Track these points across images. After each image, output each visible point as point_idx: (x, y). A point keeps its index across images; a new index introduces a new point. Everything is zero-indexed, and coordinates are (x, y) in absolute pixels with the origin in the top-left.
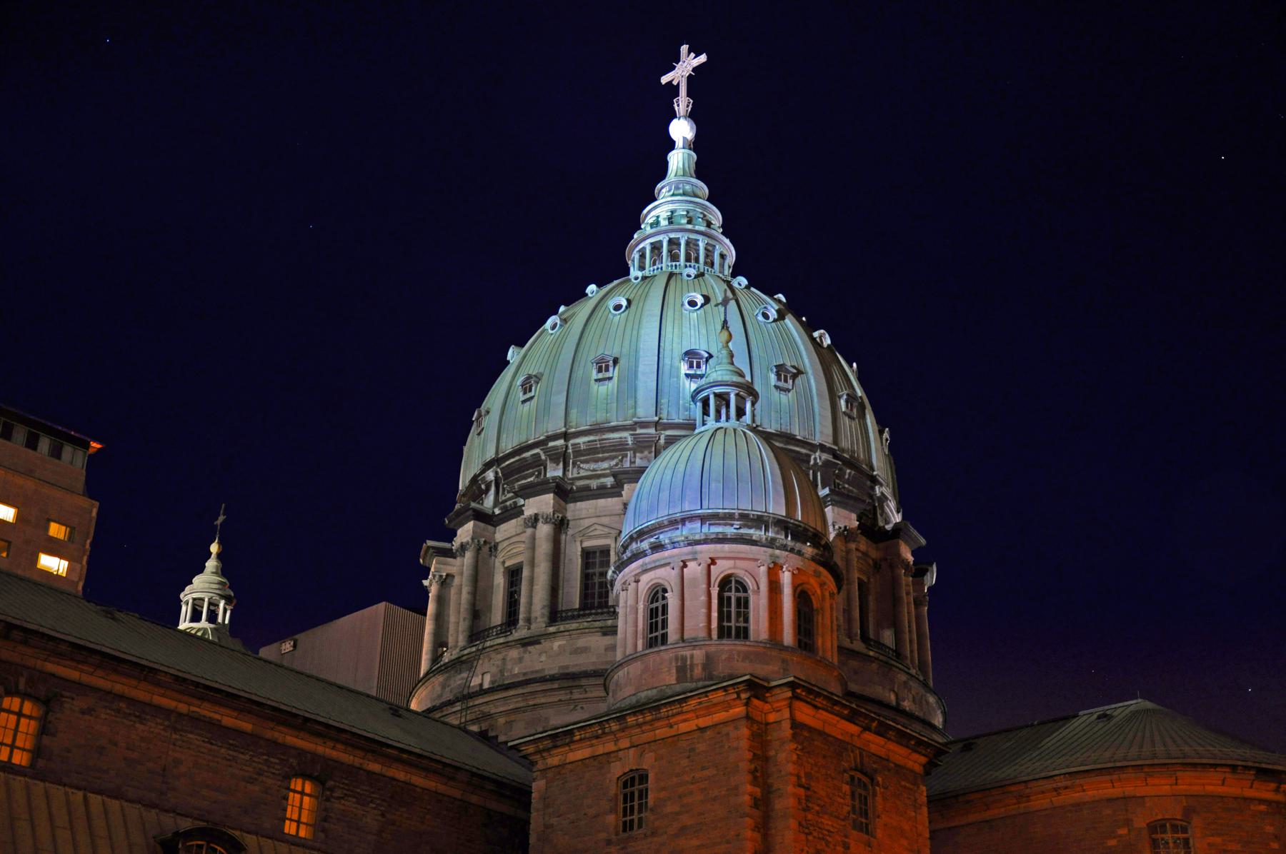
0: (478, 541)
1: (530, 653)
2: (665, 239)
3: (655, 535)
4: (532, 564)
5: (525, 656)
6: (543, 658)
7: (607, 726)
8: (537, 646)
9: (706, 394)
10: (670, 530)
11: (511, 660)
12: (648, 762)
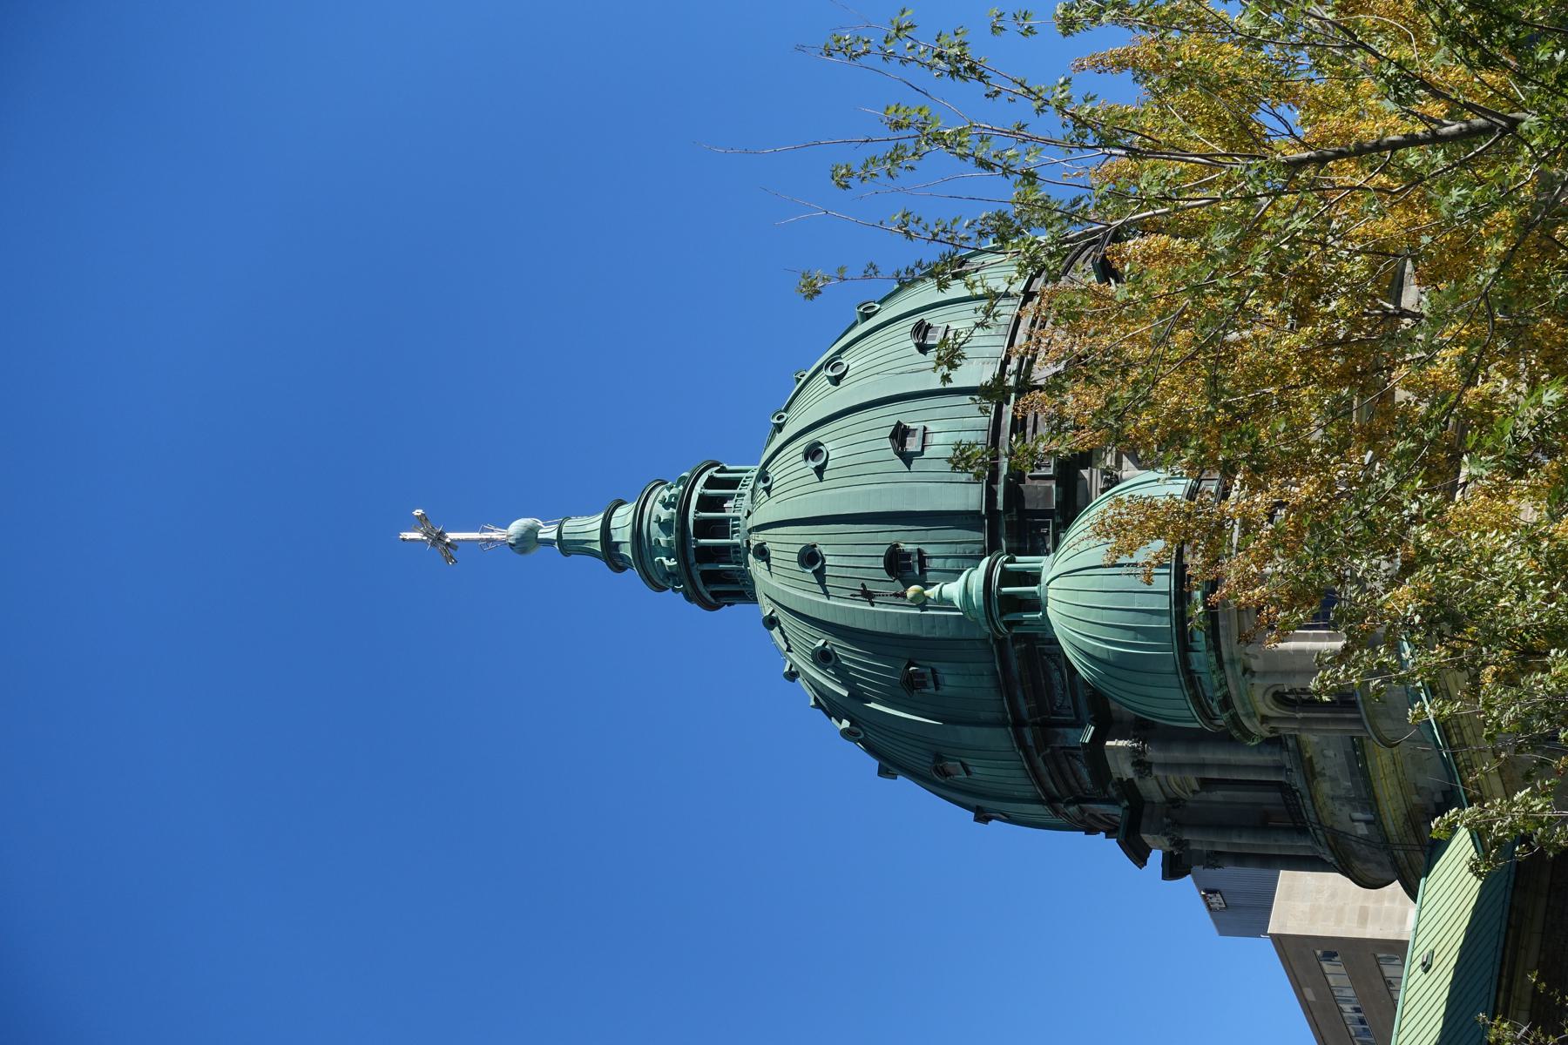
0: (1168, 825)
1: (1324, 769)
2: (697, 570)
3: (1207, 701)
4: (1203, 766)
5: (1328, 774)
6: (1330, 753)
7: (1463, 764)
8: (1315, 760)
9: (1003, 626)
10: (1201, 686)
11: (1332, 790)
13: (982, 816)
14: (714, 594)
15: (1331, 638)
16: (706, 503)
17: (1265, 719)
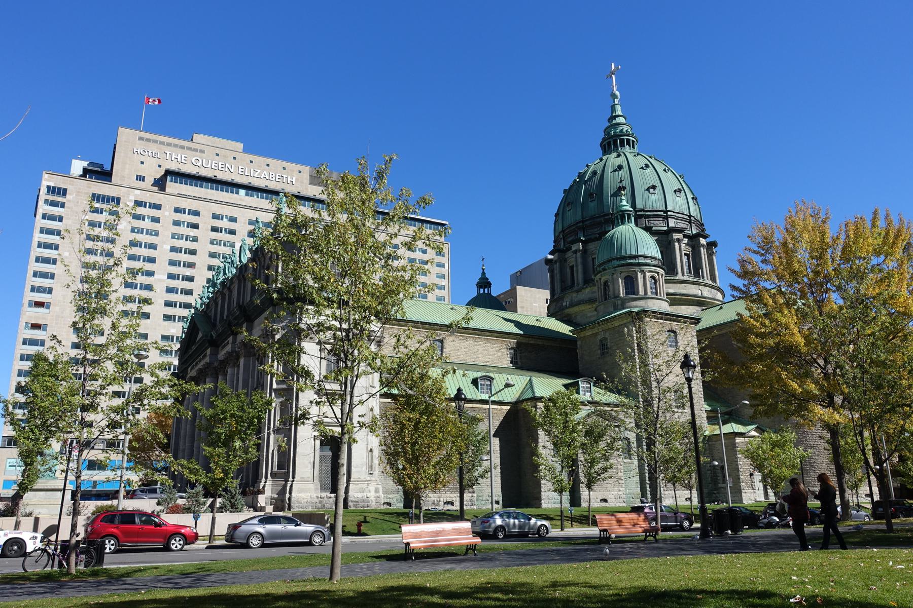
2: (611, 140)
4: (577, 266)
12: (607, 335)
13: (556, 215)
14: (605, 145)
15: (623, 294)
16: (628, 140)
17: (600, 279)
